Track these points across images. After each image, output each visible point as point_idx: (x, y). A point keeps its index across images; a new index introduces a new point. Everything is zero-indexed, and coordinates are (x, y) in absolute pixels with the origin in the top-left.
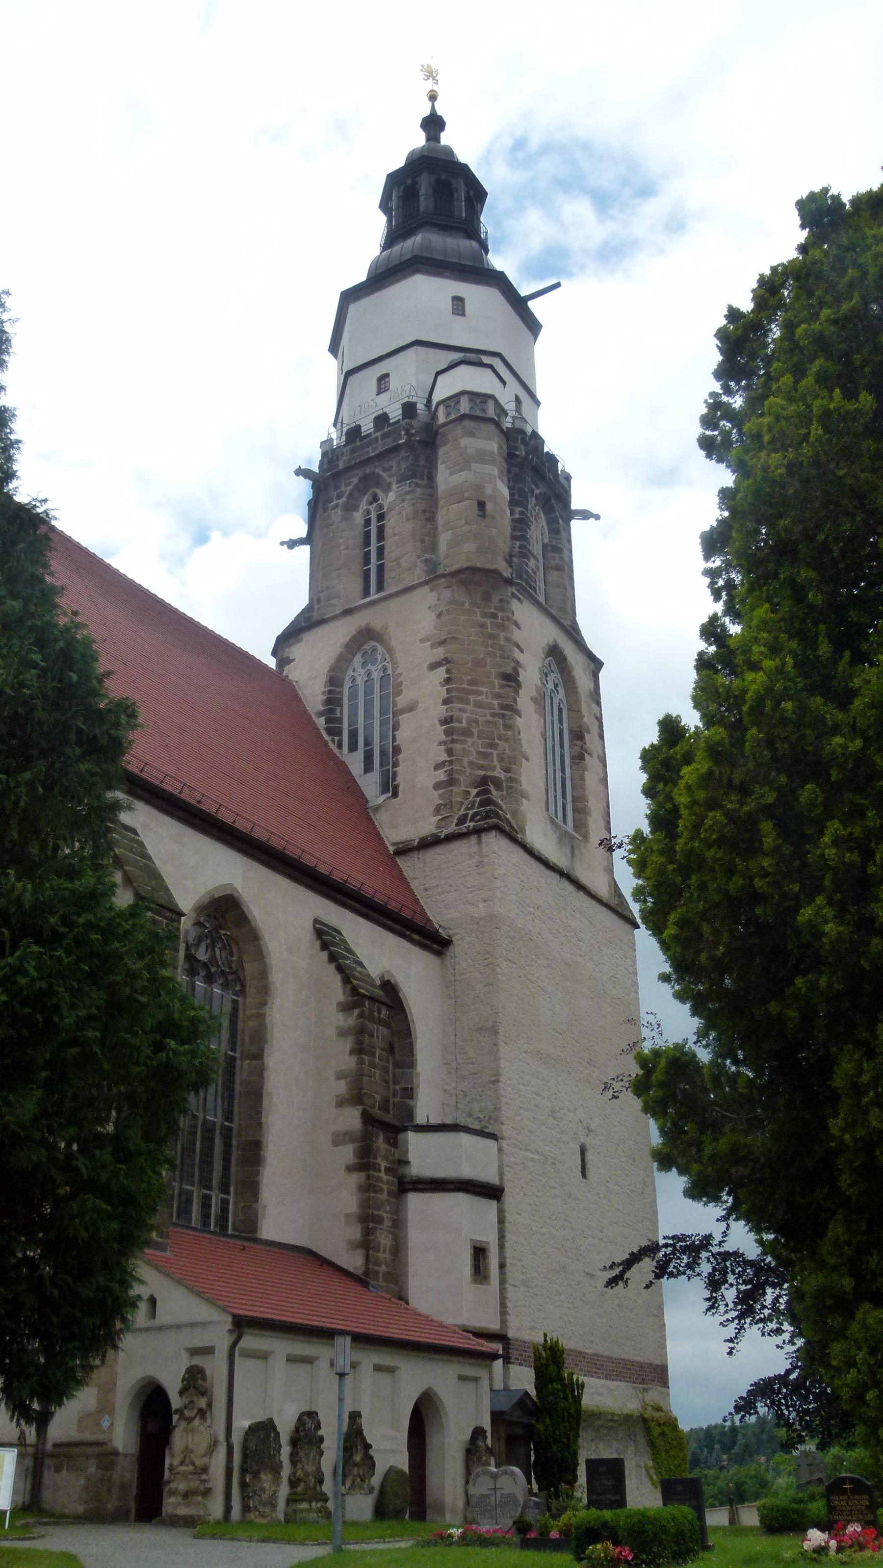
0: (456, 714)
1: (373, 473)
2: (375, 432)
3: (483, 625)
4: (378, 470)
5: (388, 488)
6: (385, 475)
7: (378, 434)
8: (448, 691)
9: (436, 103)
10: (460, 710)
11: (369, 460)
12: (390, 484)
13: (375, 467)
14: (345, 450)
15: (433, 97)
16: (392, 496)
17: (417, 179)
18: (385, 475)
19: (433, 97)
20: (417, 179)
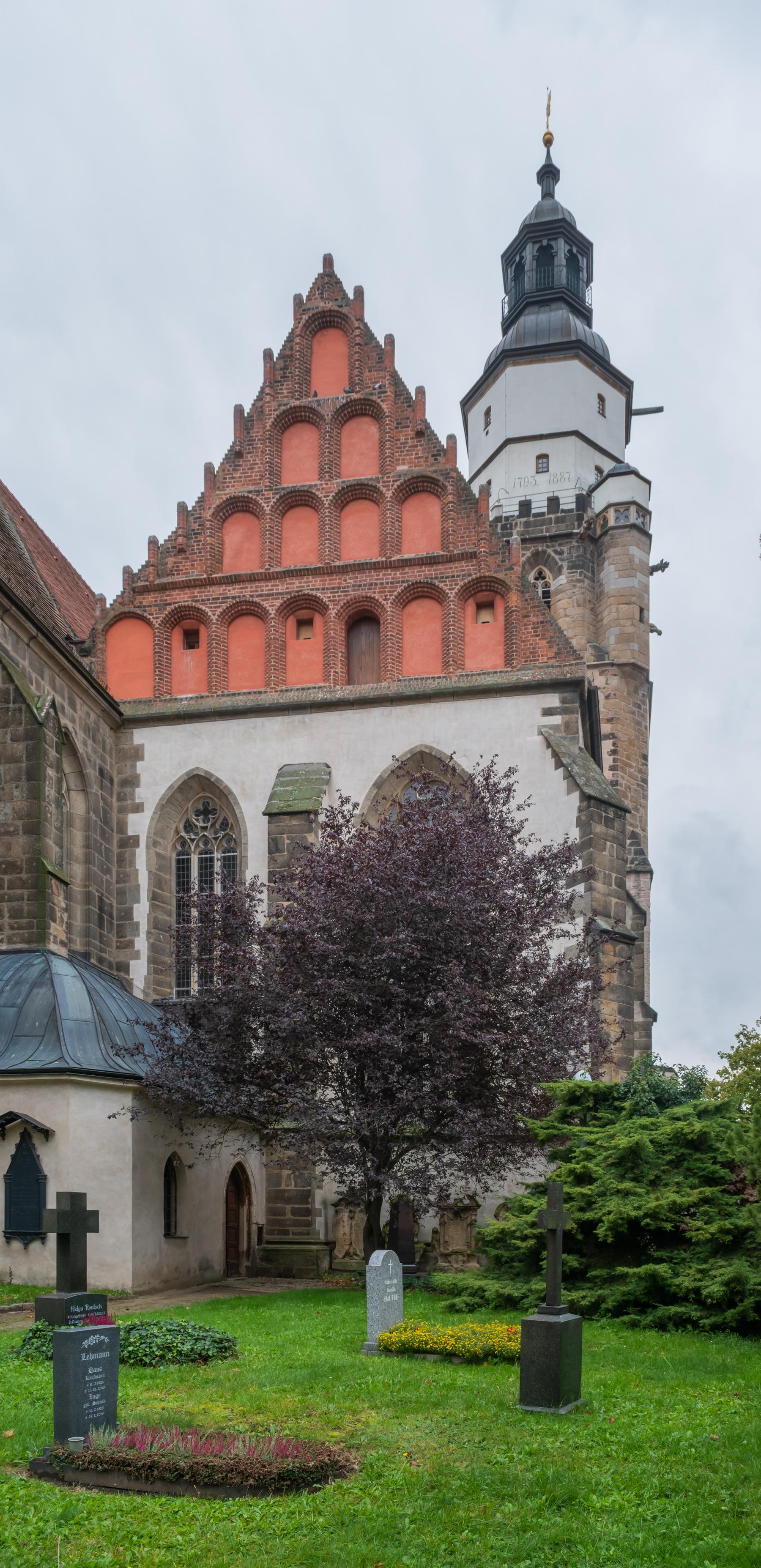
0: (620, 780)
1: (544, 552)
2: (549, 513)
3: (633, 713)
4: (550, 551)
5: (558, 572)
6: (557, 557)
7: (552, 516)
8: (615, 760)
9: (551, 149)
10: (622, 777)
11: (543, 539)
12: (560, 569)
13: (548, 547)
14: (519, 520)
15: (548, 141)
16: (563, 579)
17: (553, 243)
18: (557, 557)
19: (548, 141)
20: (553, 243)
